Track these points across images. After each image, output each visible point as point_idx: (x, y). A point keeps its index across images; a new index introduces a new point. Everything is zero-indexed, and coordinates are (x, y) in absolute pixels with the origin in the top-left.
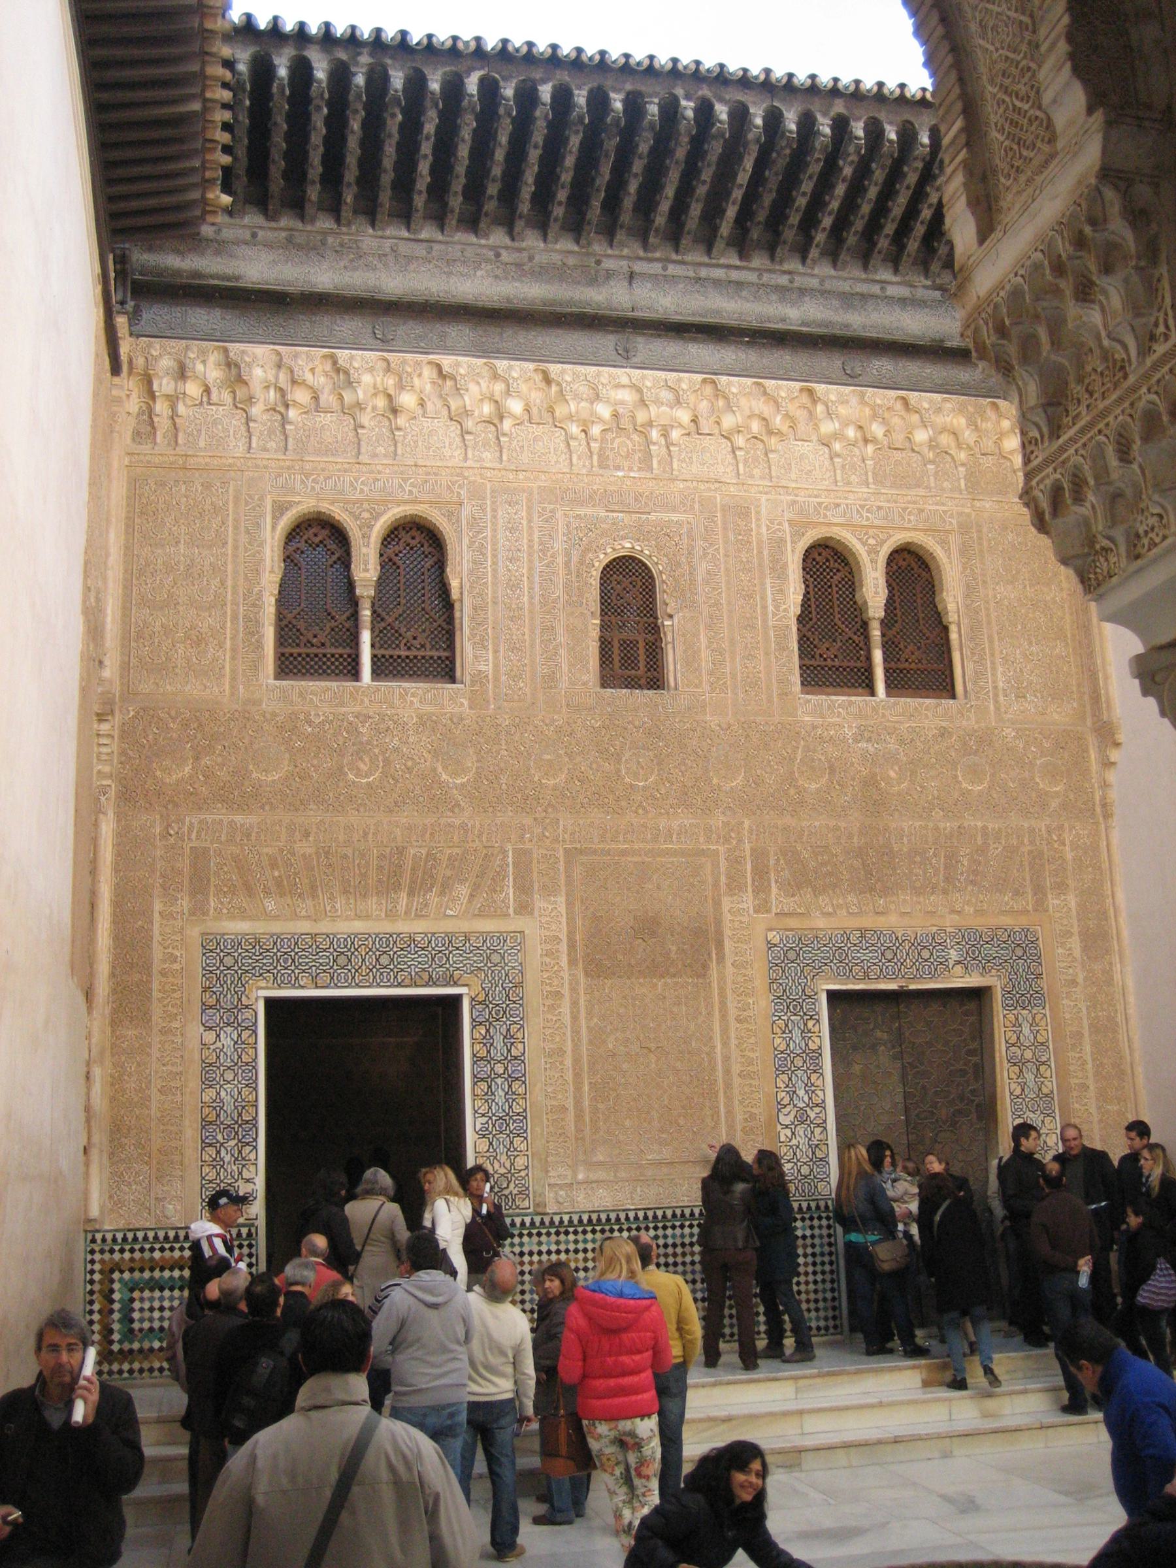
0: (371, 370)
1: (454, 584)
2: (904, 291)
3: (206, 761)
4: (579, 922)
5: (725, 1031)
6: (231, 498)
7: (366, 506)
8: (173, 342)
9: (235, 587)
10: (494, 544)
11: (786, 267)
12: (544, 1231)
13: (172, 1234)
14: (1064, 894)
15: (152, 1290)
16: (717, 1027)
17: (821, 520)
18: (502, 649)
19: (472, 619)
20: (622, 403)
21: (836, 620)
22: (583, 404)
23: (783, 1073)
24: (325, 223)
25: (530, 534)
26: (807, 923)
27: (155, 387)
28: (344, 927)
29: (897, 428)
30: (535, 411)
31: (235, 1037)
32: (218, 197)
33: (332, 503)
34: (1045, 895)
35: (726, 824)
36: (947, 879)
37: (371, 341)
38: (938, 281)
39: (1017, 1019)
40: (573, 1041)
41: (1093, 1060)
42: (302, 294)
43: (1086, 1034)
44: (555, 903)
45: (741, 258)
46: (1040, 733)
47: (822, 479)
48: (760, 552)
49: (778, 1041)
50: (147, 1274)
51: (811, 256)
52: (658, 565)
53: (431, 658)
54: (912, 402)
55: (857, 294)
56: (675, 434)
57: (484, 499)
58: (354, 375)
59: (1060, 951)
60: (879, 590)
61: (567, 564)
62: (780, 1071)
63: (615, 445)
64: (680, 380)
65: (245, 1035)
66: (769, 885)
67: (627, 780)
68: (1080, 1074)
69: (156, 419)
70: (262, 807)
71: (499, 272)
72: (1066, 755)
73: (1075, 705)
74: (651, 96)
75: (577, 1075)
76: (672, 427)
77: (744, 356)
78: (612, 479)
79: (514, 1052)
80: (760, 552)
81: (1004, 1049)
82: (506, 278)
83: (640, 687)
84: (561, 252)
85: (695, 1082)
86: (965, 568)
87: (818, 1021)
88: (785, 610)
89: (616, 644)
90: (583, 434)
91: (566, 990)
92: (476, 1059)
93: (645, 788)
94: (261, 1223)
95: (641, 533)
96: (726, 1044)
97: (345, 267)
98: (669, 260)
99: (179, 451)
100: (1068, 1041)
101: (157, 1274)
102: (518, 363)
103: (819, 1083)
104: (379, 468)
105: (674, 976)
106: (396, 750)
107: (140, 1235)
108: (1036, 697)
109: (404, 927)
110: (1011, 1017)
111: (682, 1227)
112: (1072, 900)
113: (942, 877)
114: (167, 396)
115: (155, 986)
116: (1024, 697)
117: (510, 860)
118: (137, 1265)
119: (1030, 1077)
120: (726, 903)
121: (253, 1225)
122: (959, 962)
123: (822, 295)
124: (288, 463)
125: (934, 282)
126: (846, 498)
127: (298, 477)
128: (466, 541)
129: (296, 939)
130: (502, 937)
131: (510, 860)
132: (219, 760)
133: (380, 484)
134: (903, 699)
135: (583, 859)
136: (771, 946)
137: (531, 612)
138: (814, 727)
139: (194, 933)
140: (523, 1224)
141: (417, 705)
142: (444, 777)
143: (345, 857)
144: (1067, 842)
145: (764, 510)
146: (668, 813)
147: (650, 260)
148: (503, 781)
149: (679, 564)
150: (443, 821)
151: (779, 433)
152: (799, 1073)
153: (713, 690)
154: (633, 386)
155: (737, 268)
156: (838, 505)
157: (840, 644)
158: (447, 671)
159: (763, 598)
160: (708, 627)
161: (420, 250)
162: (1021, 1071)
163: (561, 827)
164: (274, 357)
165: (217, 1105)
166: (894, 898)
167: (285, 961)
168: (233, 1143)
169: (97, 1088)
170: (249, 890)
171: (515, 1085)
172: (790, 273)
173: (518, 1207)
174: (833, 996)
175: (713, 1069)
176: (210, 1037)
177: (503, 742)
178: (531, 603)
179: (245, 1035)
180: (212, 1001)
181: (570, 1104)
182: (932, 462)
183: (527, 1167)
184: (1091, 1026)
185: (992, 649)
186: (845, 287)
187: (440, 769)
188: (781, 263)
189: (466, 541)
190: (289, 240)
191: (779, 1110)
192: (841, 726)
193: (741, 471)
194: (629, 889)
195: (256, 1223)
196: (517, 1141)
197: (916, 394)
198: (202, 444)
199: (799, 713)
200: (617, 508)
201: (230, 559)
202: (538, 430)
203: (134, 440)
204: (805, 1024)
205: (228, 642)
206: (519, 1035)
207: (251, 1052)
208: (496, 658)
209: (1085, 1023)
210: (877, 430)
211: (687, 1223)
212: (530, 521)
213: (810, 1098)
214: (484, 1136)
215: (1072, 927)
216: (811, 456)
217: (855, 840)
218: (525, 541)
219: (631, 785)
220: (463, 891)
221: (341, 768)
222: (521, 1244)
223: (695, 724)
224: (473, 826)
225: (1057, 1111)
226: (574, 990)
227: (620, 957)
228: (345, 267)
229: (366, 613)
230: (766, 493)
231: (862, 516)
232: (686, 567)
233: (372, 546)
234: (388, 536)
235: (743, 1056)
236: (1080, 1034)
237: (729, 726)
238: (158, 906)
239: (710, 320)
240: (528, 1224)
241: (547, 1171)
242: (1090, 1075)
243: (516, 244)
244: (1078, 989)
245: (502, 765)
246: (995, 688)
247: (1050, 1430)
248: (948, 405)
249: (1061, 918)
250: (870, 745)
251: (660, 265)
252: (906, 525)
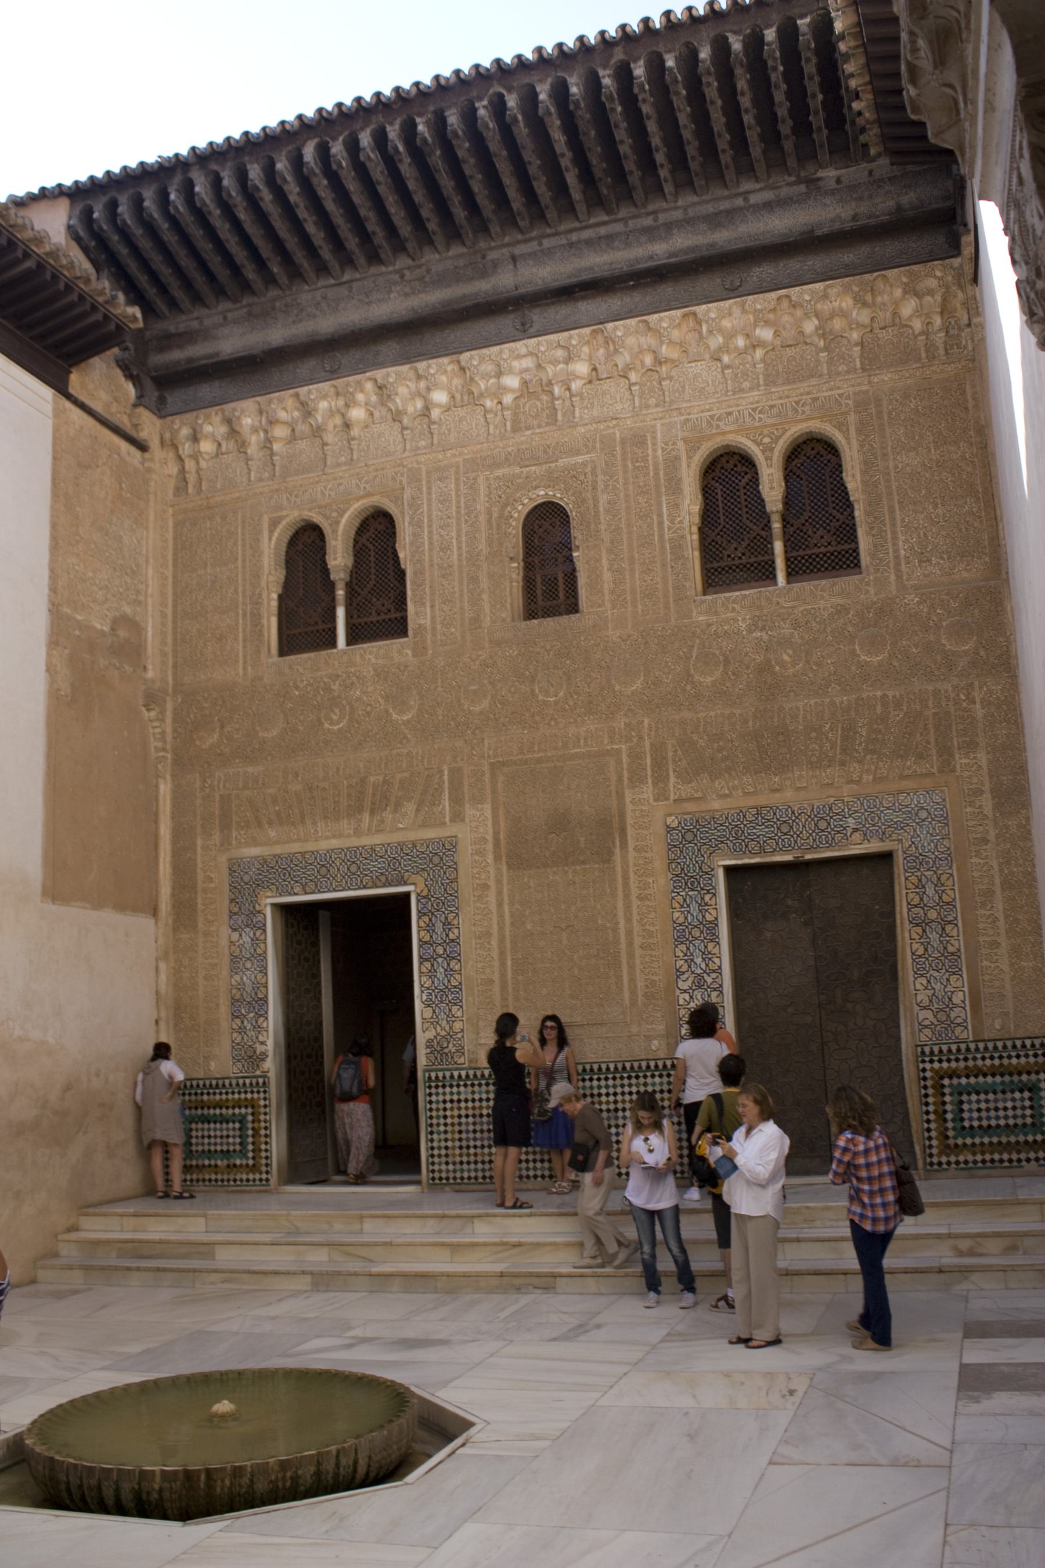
0: (325, 397)
1: (401, 555)
2: (768, 195)
3: (228, 729)
4: (502, 825)
5: (628, 907)
6: (240, 521)
7: (334, 507)
8: (188, 415)
9: (244, 591)
10: (430, 516)
11: (651, 208)
12: (476, 1082)
13: (214, 1082)
14: (974, 753)
15: (203, 1123)
16: (620, 905)
17: (714, 431)
18: (437, 603)
19: (413, 583)
20: (527, 370)
21: (744, 520)
22: (492, 381)
23: (682, 943)
24: (274, 293)
25: (458, 502)
26: (704, 807)
27: (181, 452)
28: (323, 845)
29: (788, 326)
30: (458, 396)
31: (252, 935)
32: (125, 311)
33: (310, 510)
34: (952, 755)
35: (627, 725)
36: (844, 751)
37: (323, 374)
38: (803, 174)
39: (920, 881)
40: (499, 923)
41: (1006, 917)
42: (264, 352)
43: (998, 891)
44: (482, 809)
45: (609, 212)
46: (947, 594)
47: (714, 393)
48: (657, 474)
49: (676, 915)
50: (199, 1112)
51: (666, 191)
52: (569, 508)
53: (396, 619)
54: (793, 298)
55: (721, 212)
56: (575, 386)
57: (420, 481)
58: (311, 404)
59: (969, 810)
60: (775, 485)
61: (489, 521)
62: (679, 940)
63: (527, 408)
64: (571, 337)
65: (258, 933)
66: (668, 775)
67: (540, 697)
68: (991, 932)
69: (187, 476)
70: (266, 759)
71: (407, 290)
72: (976, 611)
73: (987, 559)
74: (449, 107)
75: (502, 953)
76: (570, 380)
77: (628, 300)
78: (523, 439)
79: (451, 936)
80: (657, 474)
81: (905, 910)
82: (414, 293)
83: (560, 614)
84: (451, 258)
85: (602, 955)
86: (862, 446)
87: (714, 895)
88: (681, 522)
89: (539, 580)
90: (499, 407)
91: (492, 883)
92: (422, 943)
93: (556, 703)
94: (272, 1075)
95: (551, 480)
96: (629, 920)
97: (294, 322)
98: (540, 238)
99: (203, 496)
100: (978, 899)
101: (206, 1111)
102: (434, 361)
103: (716, 951)
104: (341, 474)
105: (583, 862)
106: (359, 699)
107: (195, 1083)
108: (942, 558)
109: (367, 841)
110: (914, 879)
111: (591, 1080)
112: (983, 758)
113: (838, 751)
114: (191, 456)
115: (199, 901)
116: (929, 561)
117: (446, 777)
118: (193, 1105)
119: (934, 937)
120: (628, 795)
121: (265, 1076)
122: (856, 830)
123: (688, 223)
124: (276, 486)
125: (798, 176)
126: (737, 405)
127: (284, 496)
128: (407, 519)
129: (291, 857)
130: (440, 842)
131: (446, 777)
132: (237, 726)
133: (342, 488)
134: (799, 584)
135: (506, 770)
136: (669, 829)
137: (460, 567)
138: (709, 625)
139: (223, 859)
140: (460, 1076)
141: (373, 660)
142: (394, 716)
143: (324, 789)
144: (978, 700)
145: (659, 435)
146: (576, 721)
147: (526, 241)
148: (440, 712)
149: (584, 501)
150: (394, 752)
151: (667, 361)
152: (697, 943)
153: (614, 607)
154: (531, 354)
155: (604, 223)
156: (730, 414)
157: (747, 542)
158: (398, 627)
159: (660, 515)
160: (609, 551)
161: (343, 291)
162: (924, 931)
163: (486, 745)
164: (257, 406)
165: (241, 986)
166: (790, 775)
167: (284, 875)
168: (252, 1015)
169: (163, 977)
170: (260, 825)
171: (453, 963)
172: (654, 212)
173: (456, 1063)
174: (729, 870)
175: (617, 942)
176: (235, 936)
177: (439, 681)
178: (460, 560)
179: (258, 933)
180: (236, 910)
181: (496, 977)
182: (826, 349)
183: (462, 1031)
184: (1002, 884)
185: (893, 519)
186: (710, 209)
187: (391, 711)
188: (644, 206)
189: (407, 519)
190: (250, 314)
191: (678, 977)
192: (736, 620)
193: (637, 404)
194: (543, 791)
195: (269, 1075)
196: (455, 1009)
197: (798, 288)
198: (219, 486)
199: (694, 614)
200: (528, 463)
201: (240, 570)
202: (461, 412)
203: (175, 495)
204: (702, 899)
205: (241, 635)
206: (455, 922)
207: (262, 945)
208: (433, 611)
209: (997, 881)
210: (766, 334)
211: (595, 1077)
212: (457, 490)
213: (707, 965)
214: (429, 1006)
215: (982, 784)
216: (704, 374)
217: (750, 724)
218: (454, 508)
219: (544, 701)
220: (410, 807)
221: (319, 720)
222: (459, 1093)
223: (598, 640)
224: (417, 753)
225: (964, 969)
226: (499, 882)
227: (537, 850)
228: (294, 322)
229: (340, 593)
230: (661, 418)
231: (754, 419)
232: (591, 502)
233: (339, 538)
234: (361, 525)
235: (644, 930)
236: (989, 893)
237: (629, 636)
238: (199, 842)
239: (585, 277)
240: (464, 1077)
241: (478, 1033)
242: (1003, 931)
243: (417, 262)
244: (989, 846)
245: (439, 699)
246: (897, 558)
247: (795, 1278)
248: (832, 292)
249: (970, 777)
250: (764, 634)
251: (535, 243)
252: (799, 417)
